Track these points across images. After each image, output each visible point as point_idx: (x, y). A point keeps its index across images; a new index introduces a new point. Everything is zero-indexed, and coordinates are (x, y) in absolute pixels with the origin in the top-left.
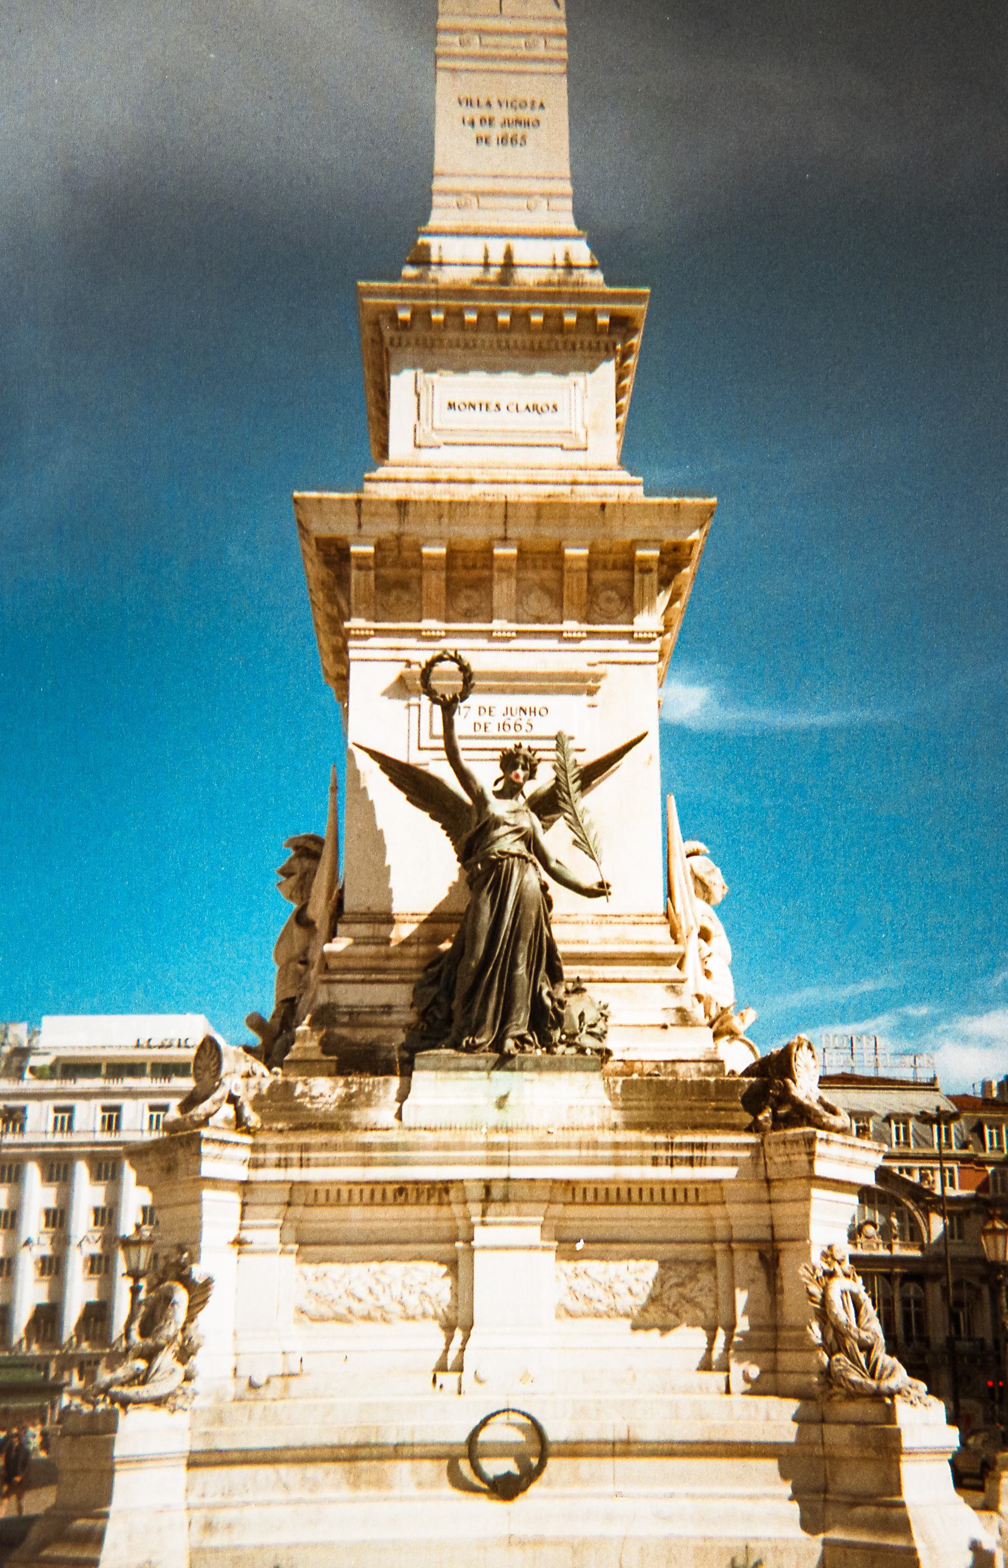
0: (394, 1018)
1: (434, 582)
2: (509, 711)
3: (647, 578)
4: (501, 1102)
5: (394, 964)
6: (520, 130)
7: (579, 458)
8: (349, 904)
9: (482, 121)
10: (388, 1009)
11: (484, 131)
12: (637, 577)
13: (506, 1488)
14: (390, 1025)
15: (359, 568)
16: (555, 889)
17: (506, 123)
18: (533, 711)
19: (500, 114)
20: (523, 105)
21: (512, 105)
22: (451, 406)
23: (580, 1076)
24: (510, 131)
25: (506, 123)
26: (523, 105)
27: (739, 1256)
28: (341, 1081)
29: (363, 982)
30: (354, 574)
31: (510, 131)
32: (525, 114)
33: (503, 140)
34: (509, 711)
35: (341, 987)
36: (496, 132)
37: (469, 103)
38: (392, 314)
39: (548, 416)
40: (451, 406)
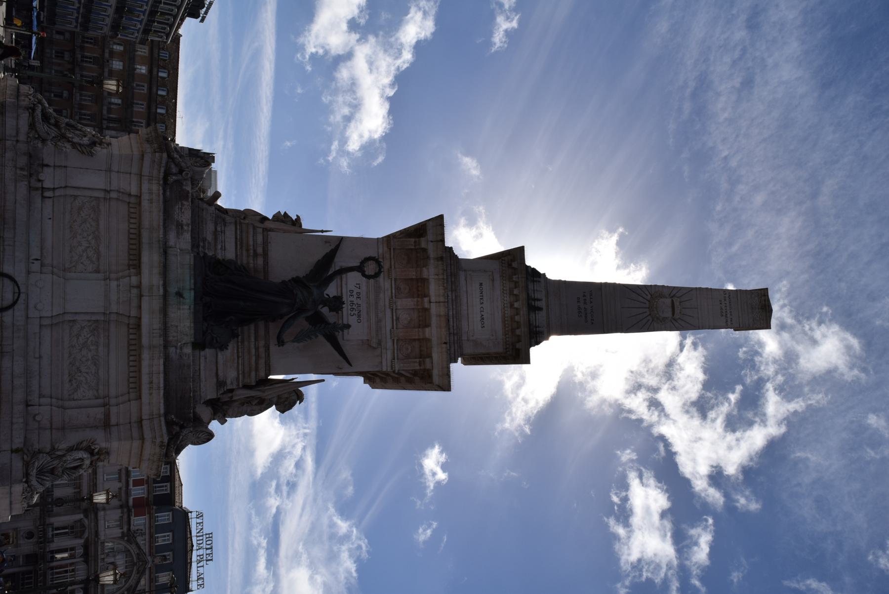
0: (219, 251)
1: (412, 274)
2: (359, 305)
3: (417, 364)
4: (179, 294)
5: (244, 252)
7: (464, 337)
9: (585, 300)
10: (224, 249)
12: (418, 360)
14: (216, 249)
15: (415, 242)
18: (359, 316)
22: (481, 284)
23: (192, 332)
27: (102, 409)
28: (189, 222)
29: (236, 238)
30: (413, 240)
33: (579, 308)
34: (359, 305)
35: (233, 228)
37: (591, 295)
40: (481, 284)
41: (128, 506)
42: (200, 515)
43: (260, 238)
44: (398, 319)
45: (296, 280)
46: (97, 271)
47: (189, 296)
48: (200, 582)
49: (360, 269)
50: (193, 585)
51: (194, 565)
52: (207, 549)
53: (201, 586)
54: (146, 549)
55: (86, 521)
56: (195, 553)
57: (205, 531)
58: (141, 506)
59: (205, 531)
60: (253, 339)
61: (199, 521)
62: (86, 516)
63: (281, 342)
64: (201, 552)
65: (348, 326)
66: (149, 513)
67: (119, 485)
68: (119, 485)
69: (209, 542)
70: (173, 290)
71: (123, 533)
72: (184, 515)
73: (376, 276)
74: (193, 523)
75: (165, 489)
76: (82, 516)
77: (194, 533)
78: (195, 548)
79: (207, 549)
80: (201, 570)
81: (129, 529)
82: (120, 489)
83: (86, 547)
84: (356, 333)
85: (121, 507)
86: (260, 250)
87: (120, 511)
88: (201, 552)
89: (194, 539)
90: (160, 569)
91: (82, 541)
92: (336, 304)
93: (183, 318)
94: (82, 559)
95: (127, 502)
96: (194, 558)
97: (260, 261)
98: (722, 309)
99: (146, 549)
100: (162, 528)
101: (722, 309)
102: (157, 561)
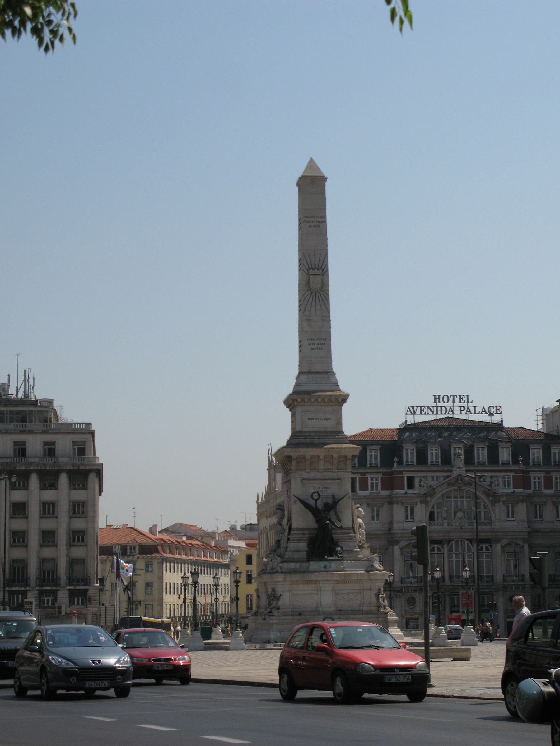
4: (325, 567)
6: (321, 346)
7: (335, 430)
8: (294, 526)
11: (313, 347)
16: (333, 527)
17: (318, 344)
19: (316, 342)
20: (322, 339)
21: (318, 339)
22: (309, 419)
24: (319, 346)
25: (318, 344)
26: (322, 339)
31: (319, 346)
32: (322, 342)
33: (317, 349)
36: (315, 347)
37: (310, 339)
38: (296, 400)
39: (329, 421)
40: (309, 419)
42: (412, 411)
43: (296, 532)
44: (328, 469)
45: (317, 522)
46: (318, 594)
48: (493, 410)
49: (316, 500)
50: (496, 419)
51: (472, 417)
52: (454, 402)
53: (498, 409)
56: (455, 416)
57: (431, 404)
59: (431, 404)
60: (337, 536)
61: (418, 412)
62: (397, 542)
63: (342, 527)
64: (457, 409)
65: (333, 496)
66: (401, 472)
69: (446, 398)
70: (323, 569)
71: (421, 502)
72: (407, 428)
73: (318, 493)
74: (420, 418)
75: (374, 454)
76: (396, 549)
77: (431, 417)
78: (451, 416)
79: (454, 402)
80: (478, 409)
81: (419, 496)
85: (391, 503)
86: (301, 532)
87: (395, 506)
88: (457, 409)
89: (440, 417)
94: (446, 545)
96: (463, 417)
97: (306, 532)
98: (314, 226)
100: (422, 458)
101: (314, 226)
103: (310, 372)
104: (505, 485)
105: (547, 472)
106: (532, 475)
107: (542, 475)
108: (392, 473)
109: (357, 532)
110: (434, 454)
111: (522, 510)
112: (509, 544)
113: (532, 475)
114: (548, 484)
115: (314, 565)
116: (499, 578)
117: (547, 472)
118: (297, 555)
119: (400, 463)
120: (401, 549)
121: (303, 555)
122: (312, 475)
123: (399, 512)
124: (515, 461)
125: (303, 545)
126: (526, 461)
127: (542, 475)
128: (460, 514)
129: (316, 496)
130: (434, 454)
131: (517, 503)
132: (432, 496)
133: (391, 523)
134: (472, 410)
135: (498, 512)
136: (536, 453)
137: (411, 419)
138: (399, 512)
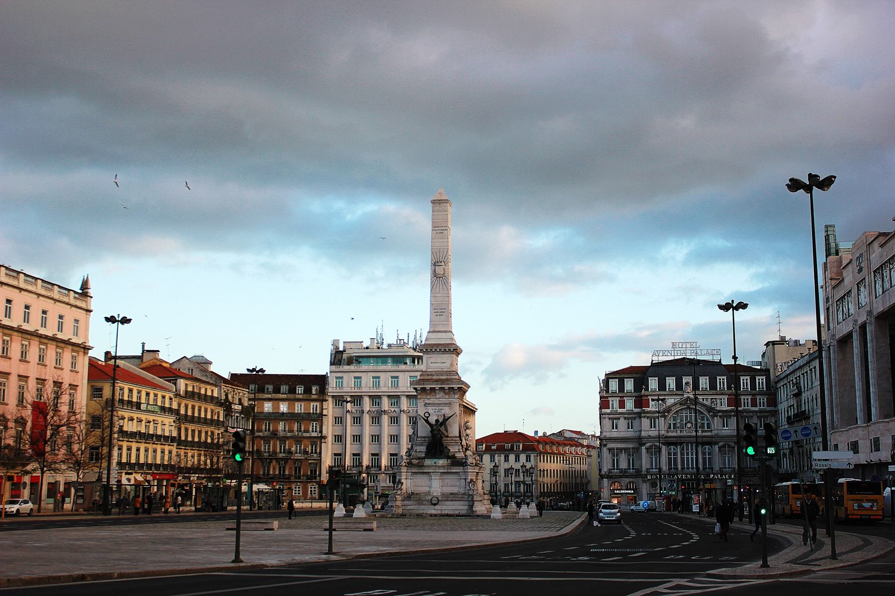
13: (435, 505)
41: (640, 413)
47: (436, 460)
50: (716, 359)
54: (678, 398)
55: (648, 445)
58: (640, 402)
62: (645, 444)
67: (622, 420)
68: (622, 420)
76: (643, 448)
81: (659, 412)
82: (625, 418)
83: (668, 444)
84: (447, 411)
85: (640, 417)
89: (676, 358)
90: (696, 386)
91: (664, 448)
92: (437, 421)
93: (441, 462)
95: (637, 413)
99: (678, 398)
100: (662, 386)
102: (690, 389)
103: (434, 332)
104: (723, 405)
105: (753, 395)
106: (742, 397)
107: (750, 398)
108: (642, 396)
109: (463, 439)
110: (671, 382)
111: (733, 421)
112: (724, 446)
113: (742, 397)
114: (754, 404)
115: (428, 462)
116: (716, 468)
117: (753, 395)
118: (420, 455)
119: (647, 389)
120: (647, 449)
121: (423, 455)
122: (431, 401)
123: (645, 422)
124: (729, 388)
125: (423, 449)
126: (738, 387)
127: (750, 398)
128: (689, 425)
129: (427, 415)
130: (671, 382)
131: (730, 416)
132: (668, 412)
133: (641, 431)
134: (699, 352)
135: (716, 422)
136: (745, 380)
137: (656, 359)
138: (645, 422)
